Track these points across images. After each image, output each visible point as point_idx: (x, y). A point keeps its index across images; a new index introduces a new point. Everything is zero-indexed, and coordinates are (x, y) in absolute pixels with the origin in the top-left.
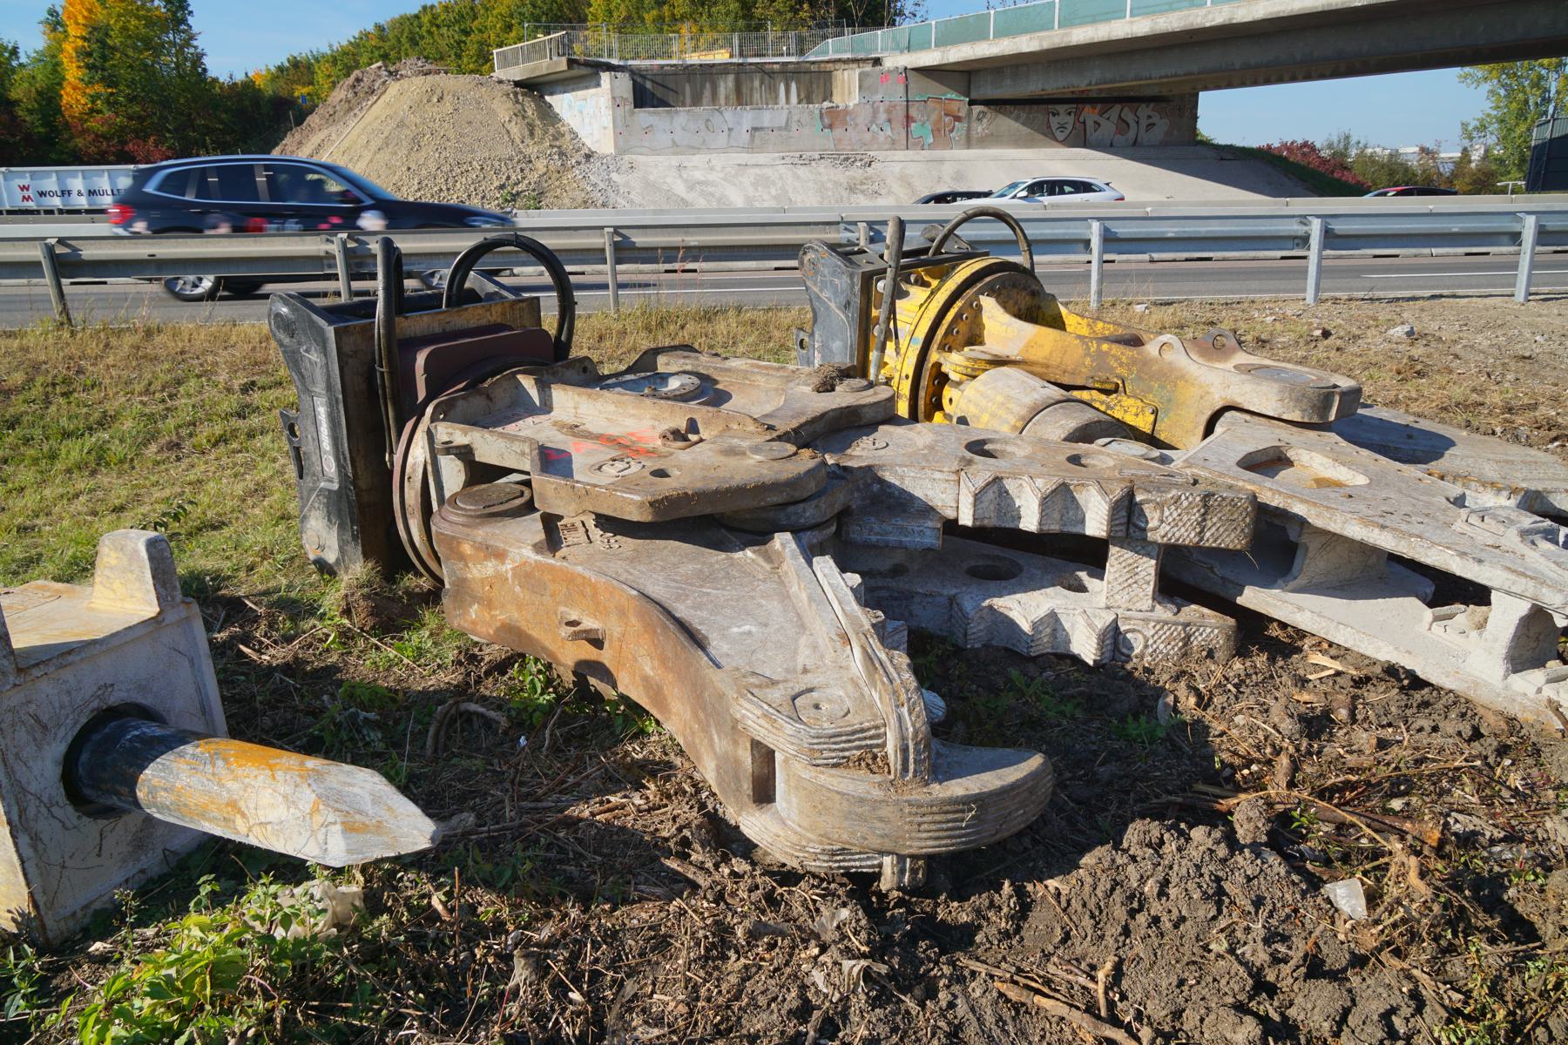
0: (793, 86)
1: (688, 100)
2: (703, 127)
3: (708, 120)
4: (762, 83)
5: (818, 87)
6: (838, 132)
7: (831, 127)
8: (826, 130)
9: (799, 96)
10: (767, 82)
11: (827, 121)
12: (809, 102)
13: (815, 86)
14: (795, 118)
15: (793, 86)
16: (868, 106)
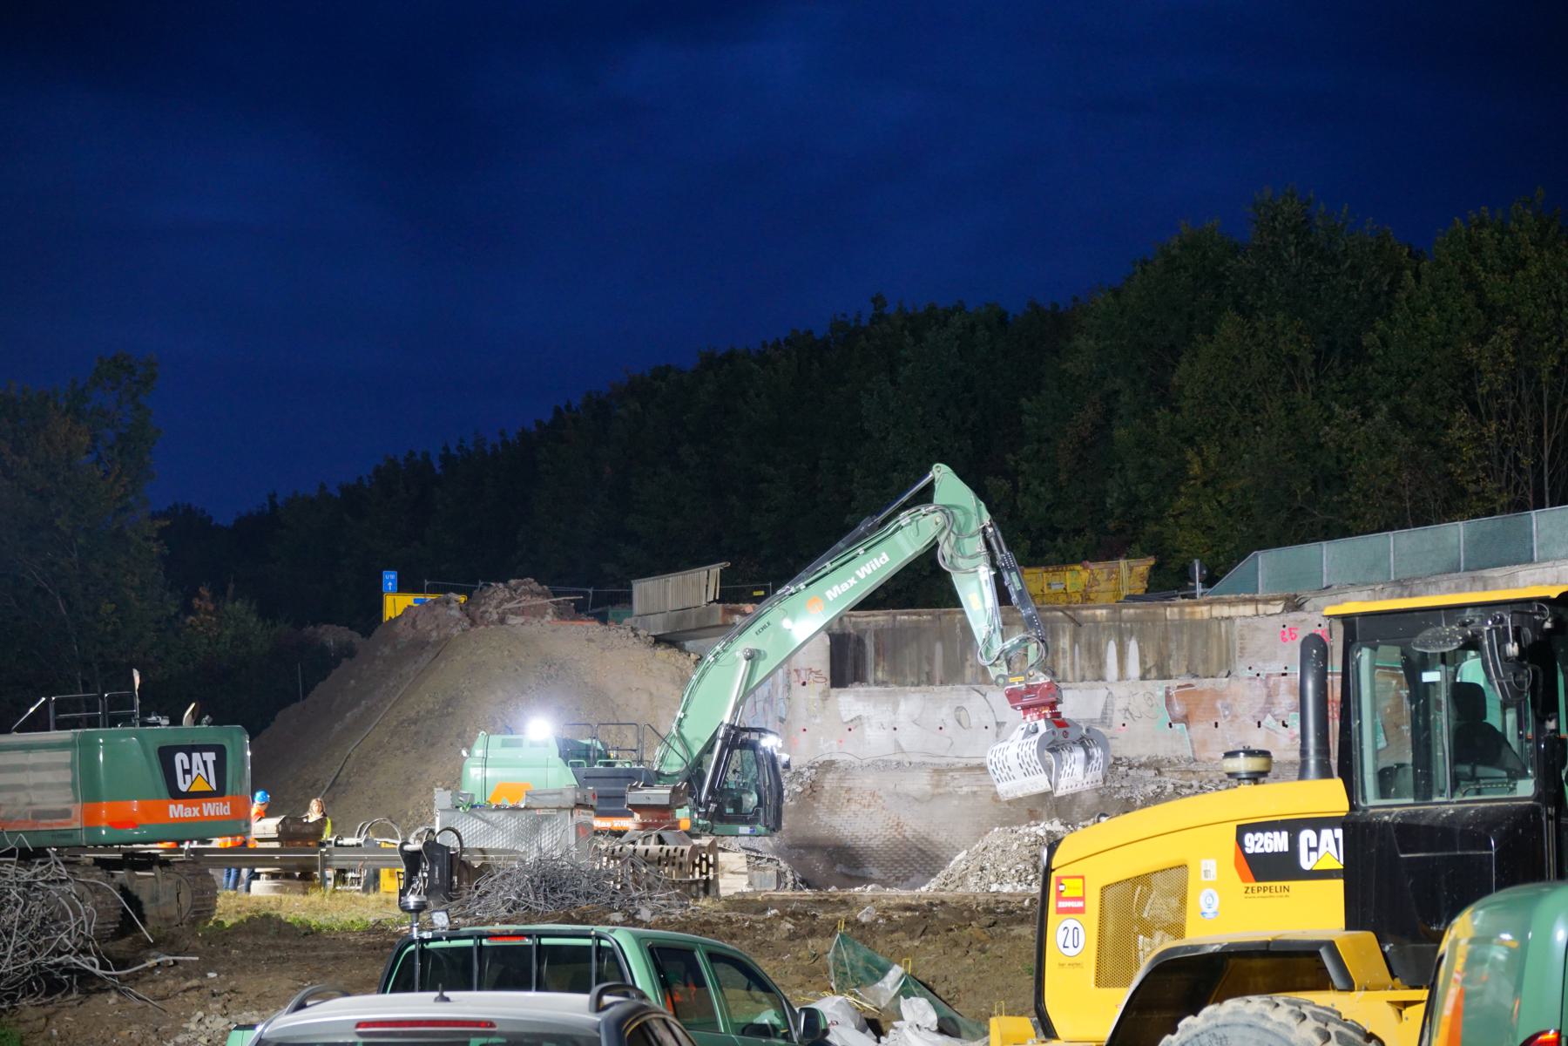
0: (1133, 647)
1: (938, 672)
2: (951, 722)
3: (959, 708)
4: (1075, 639)
5: (1179, 647)
6: (1201, 729)
7: (1185, 719)
8: (1177, 726)
9: (1142, 662)
10: (1083, 640)
11: (1178, 709)
12: (1164, 675)
13: (1173, 646)
14: (1120, 704)
15: (1133, 647)
16: (1258, 682)
